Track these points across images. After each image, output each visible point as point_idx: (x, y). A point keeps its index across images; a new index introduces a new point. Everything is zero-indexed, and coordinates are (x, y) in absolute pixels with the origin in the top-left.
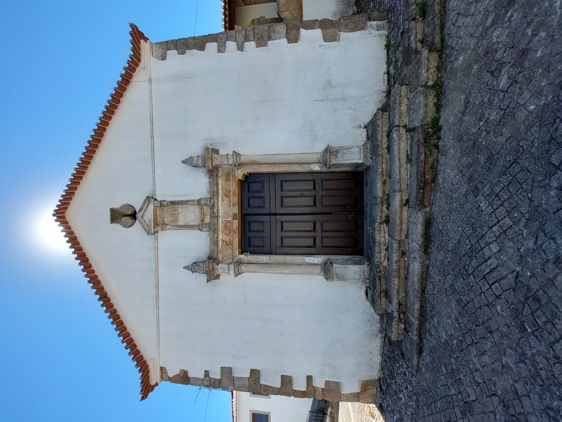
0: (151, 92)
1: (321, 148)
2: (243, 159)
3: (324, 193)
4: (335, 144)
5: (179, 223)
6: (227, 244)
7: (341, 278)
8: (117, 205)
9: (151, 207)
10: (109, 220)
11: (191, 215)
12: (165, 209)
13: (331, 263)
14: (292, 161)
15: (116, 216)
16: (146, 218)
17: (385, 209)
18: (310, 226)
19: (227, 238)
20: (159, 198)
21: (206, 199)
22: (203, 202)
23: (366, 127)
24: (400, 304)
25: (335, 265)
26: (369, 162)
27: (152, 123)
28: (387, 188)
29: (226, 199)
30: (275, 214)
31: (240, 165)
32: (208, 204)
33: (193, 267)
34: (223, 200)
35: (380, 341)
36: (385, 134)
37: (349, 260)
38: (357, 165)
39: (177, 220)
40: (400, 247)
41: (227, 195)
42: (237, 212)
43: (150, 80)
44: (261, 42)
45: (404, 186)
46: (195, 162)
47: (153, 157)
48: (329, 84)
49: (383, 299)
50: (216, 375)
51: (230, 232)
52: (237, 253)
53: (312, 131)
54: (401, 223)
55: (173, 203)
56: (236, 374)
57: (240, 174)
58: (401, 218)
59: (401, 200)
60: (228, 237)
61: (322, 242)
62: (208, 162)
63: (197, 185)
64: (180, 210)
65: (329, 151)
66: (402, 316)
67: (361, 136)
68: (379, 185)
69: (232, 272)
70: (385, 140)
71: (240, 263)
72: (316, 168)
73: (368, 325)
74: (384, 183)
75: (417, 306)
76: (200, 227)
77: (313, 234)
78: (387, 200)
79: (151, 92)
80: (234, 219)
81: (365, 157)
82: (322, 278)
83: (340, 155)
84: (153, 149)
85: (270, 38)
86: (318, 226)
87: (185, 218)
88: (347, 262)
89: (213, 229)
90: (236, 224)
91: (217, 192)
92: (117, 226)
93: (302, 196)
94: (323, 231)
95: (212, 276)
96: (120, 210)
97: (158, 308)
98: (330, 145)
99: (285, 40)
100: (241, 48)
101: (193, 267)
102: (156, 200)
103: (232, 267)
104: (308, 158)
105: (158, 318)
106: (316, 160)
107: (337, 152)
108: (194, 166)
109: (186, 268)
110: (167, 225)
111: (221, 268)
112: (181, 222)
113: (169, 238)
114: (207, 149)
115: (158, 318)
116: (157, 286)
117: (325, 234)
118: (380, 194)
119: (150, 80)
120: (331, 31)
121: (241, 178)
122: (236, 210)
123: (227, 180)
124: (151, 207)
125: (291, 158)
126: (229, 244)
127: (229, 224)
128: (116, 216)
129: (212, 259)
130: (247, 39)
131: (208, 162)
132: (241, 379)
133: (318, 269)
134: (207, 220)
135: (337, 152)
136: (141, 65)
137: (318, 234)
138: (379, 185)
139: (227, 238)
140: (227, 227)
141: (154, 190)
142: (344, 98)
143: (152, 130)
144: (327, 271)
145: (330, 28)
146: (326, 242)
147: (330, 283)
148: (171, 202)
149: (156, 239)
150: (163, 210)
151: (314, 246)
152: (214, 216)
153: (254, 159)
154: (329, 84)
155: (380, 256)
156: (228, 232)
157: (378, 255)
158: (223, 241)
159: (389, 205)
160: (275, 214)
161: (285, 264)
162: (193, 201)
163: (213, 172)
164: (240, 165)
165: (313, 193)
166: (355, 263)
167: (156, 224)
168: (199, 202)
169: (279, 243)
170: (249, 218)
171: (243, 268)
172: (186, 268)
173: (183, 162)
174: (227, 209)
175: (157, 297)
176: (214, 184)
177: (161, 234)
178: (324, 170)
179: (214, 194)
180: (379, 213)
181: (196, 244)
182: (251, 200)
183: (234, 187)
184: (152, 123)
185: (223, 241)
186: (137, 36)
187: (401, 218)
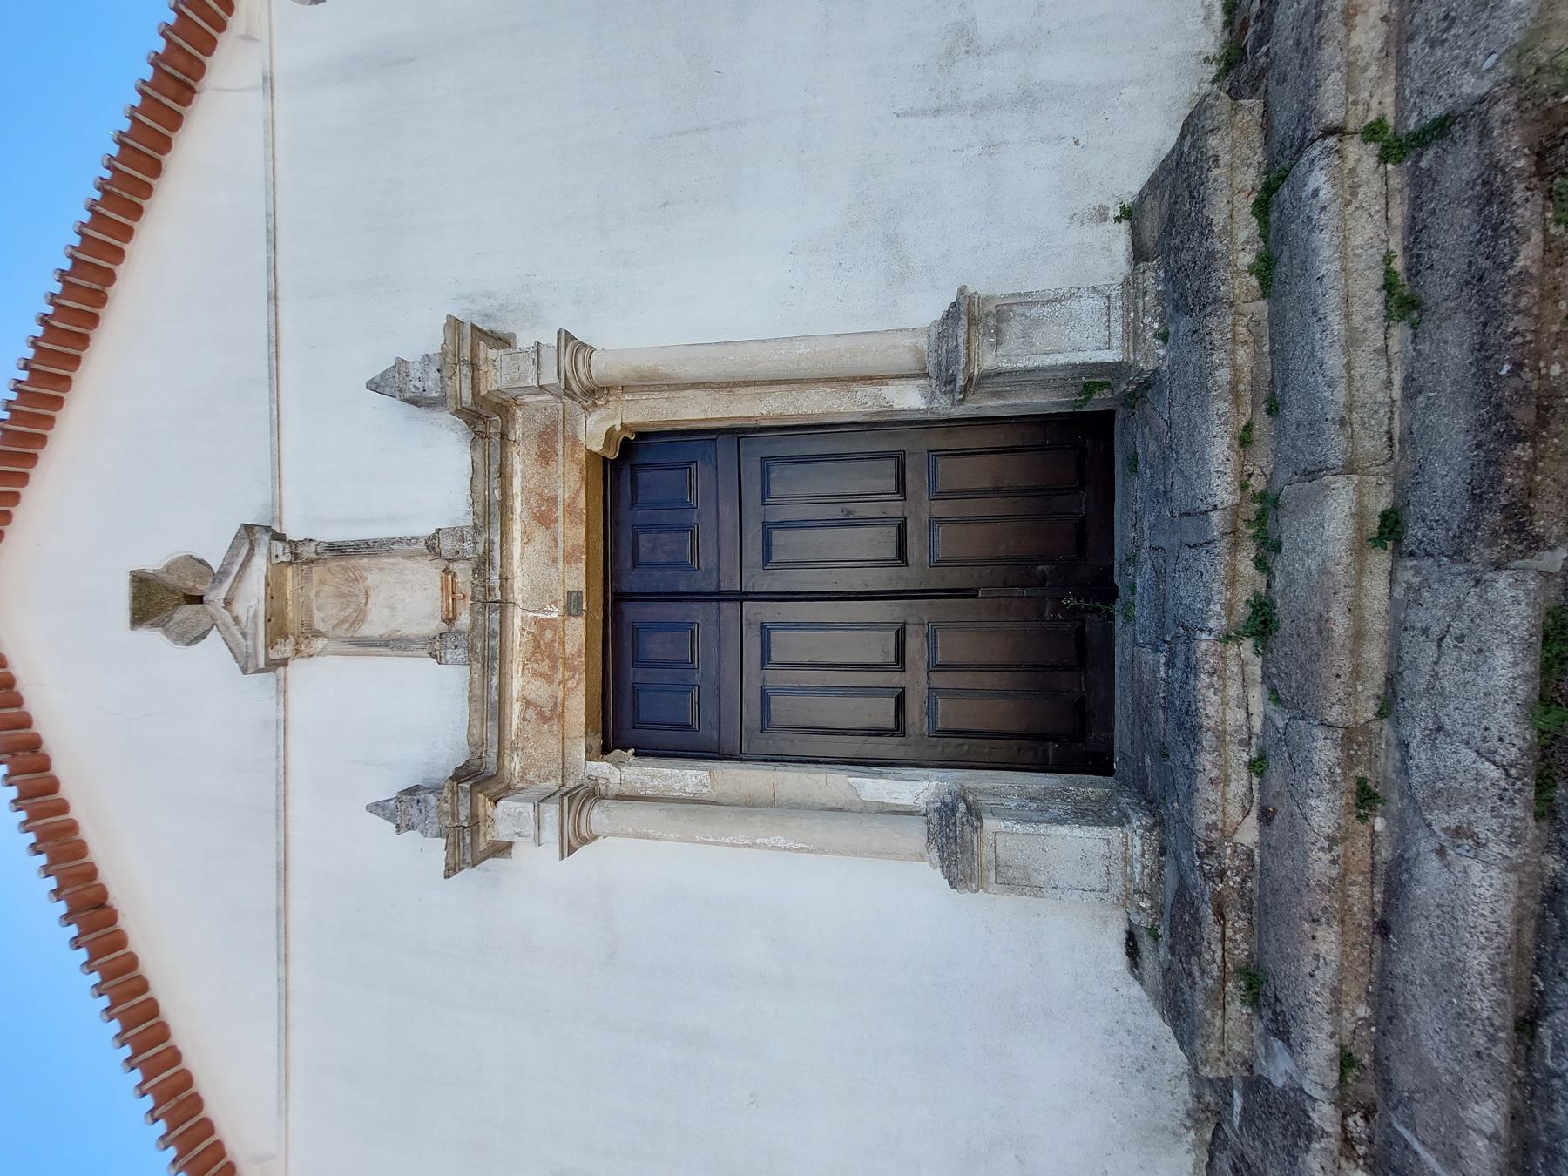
0: (271, 124)
1: (928, 308)
2: (602, 367)
3: (940, 508)
4: (990, 283)
5: (366, 631)
6: (544, 718)
7: (1018, 882)
8: (153, 561)
9: (260, 564)
10: (126, 616)
11: (410, 597)
12: (317, 572)
13: (974, 812)
14: (807, 369)
16: (240, 608)
17: (1246, 567)
18: (879, 648)
19: (541, 692)
21: (459, 534)
22: (447, 545)
23: (1127, 214)
24: (1346, 1061)
25: (990, 824)
26: (1153, 356)
27: (273, 243)
28: (1262, 459)
29: (539, 534)
30: (741, 597)
31: (595, 393)
33: (404, 808)
34: (528, 539)
35: (1190, 1160)
36: (1245, 204)
37: (1052, 794)
38: (1091, 377)
39: (360, 617)
40: (1349, 762)
41: (544, 519)
42: (583, 588)
43: (268, 82)
45: (1372, 445)
47: (275, 375)
48: (964, 42)
49: (1237, 1009)
51: (554, 667)
52: (579, 751)
53: (892, 240)
54: (1359, 636)
55: (338, 550)
57: (595, 430)
58: (1354, 609)
59: (1359, 515)
60: (550, 685)
61: (931, 713)
62: (468, 380)
63: (428, 479)
64: (372, 579)
65: (968, 315)
66: (1356, 1123)
68: (1220, 449)
69: (551, 835)
70: (1247, 229)
71: (592, 794)
72: (908, 399)
73: (1137, 1088)
74: (1245, 439)
75: (1487, 1113)
76: (434, 647)
77: (894, 679)
78: (1265, 523)
79: (271, 124)
80: (569, 612)
81: (1133, 334)
82: (930, 875)
83: (1013, 330)
84: (275, 342)
86: (914, 645)
87: (392, 608)
88: (1041, 811)
90: (576, 633)
91: (505, 506)
92: (151, 639)
93: (848, 522)
94: (934, 667)
95: (470, 847)
96: (172, 580)
97: (284, 958)
98: (971, 290)
102: (280, 537)
103: (551, 812)
104: (872, 363)
105: (285, 998)
106: (907, 362)
107: (1001, 316)
108: (413, 402)
109: (377, 808)
110: (317, 634)
112: (373, 627)
114: (454, 324)
115: (285, 998)
116: (283, 871)
117: (941, 680)
118: (1224, 492)
119: (268, 82)
121: (597, 446)
122: (576, 578)
123: (546, 457)
124: (260, 564)
125: (799, 357)
126: (553, 715)
127: (549, 634)
129: (477, 777)
131: (468, 380)
133: (915, 834)
135: (1001, 316)
137: (915, 680)
138: (1220, 449)
140: (543, 648)
141: (277, 504)
142: (1028, 98)
143: (273, 269)
144: (953, 840)
146: (950, 713)
147: (964, 896)
148: (331, 547)
149: (283, 691)
150: (307, 579)
151: (899, 728)
152: (492, 602)
153: (646, 362)
154: (964, 42)
155: (1224, 800)
156: (545, 666)
157: (1207, 793)
158: (527, 703)
159: (1269, 549)
160: (741, 597)
161: (774, 806)
162: (411, 541)
163: (486, 419)
164: (595, 393)
165: (895, 509)
166: (1084, 815)
167: (277, 629)
168: (432, 546)
169: (753, 714)
170: (633, 612)
171: (599, 817)
172: (377, 808)
173: (374, 386)
174: (547, 571)
175: (282, 912)
176: (492, 474)
177: (297, 670)
178: (945, 407)
179: (491, 511)
180: (1222, 585)
181: (415, 712)
182: (643, 537)
183: (570, 485)
184: (273, 243)
185: (527, 703)
187: (1354, 609)
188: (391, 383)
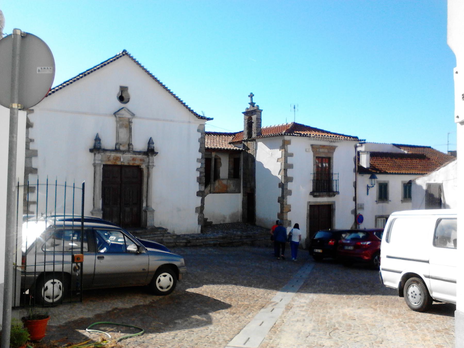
15: (123, 89)
19: (112, 158)
20: (134, 120)
27: (171, 121)
29: (132, 159)
32: (130, 148)
33: (98, 139)
41: (134, 159)
44: (199, 180)
46: (151, 145)
50: (32, 146)
52: (104, 163)
56: (34, 159)
57: (144, 166)
63: (140, 144)
67: (157, 225)
72: (144, 205)
81: (149, 226)
85: (200, 183)
89: (117, 150)
90: (119, 163)
99: (198, 190)
100: (197, 169)
101: (98, 139)
106: (149, 204)
111: (99, 156)
113: (111, 123)
120: (199, 210)
123: (141, 160)
128: (123, 89)
130: (201, 173)
131: (151, 151)
132: (31, 162)
134: (122, 148)
136: (197, 119)
139: (112, 158)
145: (201, 210)
152: (124, 152)
158: (110, 156)
172: (97, 134)
174: (125, 159)
176: (139, 153)
183: (137, 163)
184: (171, 121)
185: (110, 156)
186: (208, 119)
188: (150, 142)
